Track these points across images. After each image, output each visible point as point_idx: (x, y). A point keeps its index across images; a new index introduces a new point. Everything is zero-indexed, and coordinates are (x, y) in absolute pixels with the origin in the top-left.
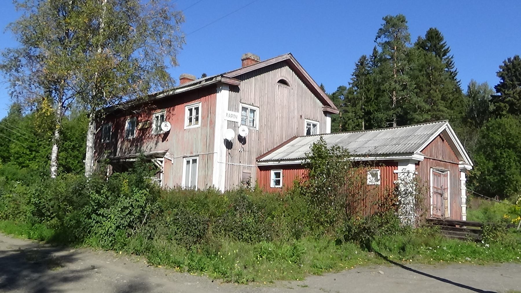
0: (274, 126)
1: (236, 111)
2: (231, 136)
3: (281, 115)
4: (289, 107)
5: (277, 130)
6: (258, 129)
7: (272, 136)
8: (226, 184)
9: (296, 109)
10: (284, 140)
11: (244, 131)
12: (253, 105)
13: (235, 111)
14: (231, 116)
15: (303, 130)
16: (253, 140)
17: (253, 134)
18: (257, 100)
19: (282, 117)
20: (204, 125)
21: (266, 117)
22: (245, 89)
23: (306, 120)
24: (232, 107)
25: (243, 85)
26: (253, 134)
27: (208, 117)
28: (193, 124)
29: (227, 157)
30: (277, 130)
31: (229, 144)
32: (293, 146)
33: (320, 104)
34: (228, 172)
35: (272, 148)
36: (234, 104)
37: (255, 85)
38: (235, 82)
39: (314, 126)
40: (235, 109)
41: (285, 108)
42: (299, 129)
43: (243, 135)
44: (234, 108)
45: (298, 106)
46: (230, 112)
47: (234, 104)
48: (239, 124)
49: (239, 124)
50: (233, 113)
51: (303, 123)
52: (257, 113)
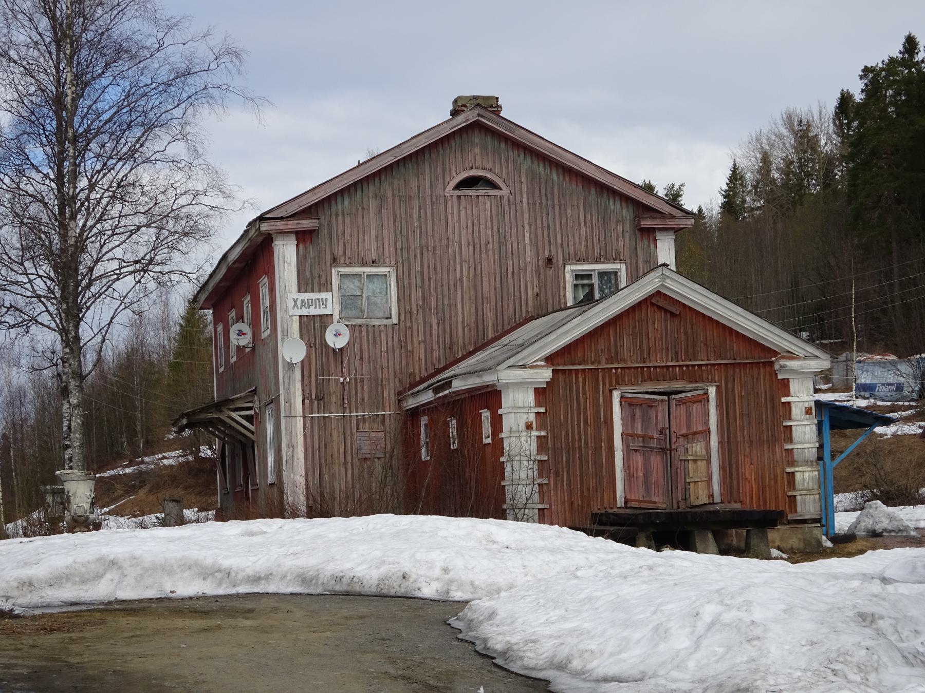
0: (452, 304)
3: (472, 271)
6: (395, 319)
7: (445, 331)
8: (310, 463)
9: (528, 248)
10: (491, 335)
11: (337, 334)
12: (374, 263)
13: (320, 291)
14: (303, 304)
16: (384, 348)
18: (389, 249)
19: (476, 278)
20: (271, 332)
21: (423, 287)
22: (348, 231)
23: (568, 268)
29: (307, 401)
30: (463, 312)
34: (313, 436)
35: (449, 360)
36: (316, 275)
37: (379, 214)
38: (305, 224)
40: (320, 284)
41: (487, 250)
42: (542, 295)
44: (316, 280)
45: (534, 236)
46: (306, 296)
47: (316, 275)
48: (336, 317)
49: (336, 317)
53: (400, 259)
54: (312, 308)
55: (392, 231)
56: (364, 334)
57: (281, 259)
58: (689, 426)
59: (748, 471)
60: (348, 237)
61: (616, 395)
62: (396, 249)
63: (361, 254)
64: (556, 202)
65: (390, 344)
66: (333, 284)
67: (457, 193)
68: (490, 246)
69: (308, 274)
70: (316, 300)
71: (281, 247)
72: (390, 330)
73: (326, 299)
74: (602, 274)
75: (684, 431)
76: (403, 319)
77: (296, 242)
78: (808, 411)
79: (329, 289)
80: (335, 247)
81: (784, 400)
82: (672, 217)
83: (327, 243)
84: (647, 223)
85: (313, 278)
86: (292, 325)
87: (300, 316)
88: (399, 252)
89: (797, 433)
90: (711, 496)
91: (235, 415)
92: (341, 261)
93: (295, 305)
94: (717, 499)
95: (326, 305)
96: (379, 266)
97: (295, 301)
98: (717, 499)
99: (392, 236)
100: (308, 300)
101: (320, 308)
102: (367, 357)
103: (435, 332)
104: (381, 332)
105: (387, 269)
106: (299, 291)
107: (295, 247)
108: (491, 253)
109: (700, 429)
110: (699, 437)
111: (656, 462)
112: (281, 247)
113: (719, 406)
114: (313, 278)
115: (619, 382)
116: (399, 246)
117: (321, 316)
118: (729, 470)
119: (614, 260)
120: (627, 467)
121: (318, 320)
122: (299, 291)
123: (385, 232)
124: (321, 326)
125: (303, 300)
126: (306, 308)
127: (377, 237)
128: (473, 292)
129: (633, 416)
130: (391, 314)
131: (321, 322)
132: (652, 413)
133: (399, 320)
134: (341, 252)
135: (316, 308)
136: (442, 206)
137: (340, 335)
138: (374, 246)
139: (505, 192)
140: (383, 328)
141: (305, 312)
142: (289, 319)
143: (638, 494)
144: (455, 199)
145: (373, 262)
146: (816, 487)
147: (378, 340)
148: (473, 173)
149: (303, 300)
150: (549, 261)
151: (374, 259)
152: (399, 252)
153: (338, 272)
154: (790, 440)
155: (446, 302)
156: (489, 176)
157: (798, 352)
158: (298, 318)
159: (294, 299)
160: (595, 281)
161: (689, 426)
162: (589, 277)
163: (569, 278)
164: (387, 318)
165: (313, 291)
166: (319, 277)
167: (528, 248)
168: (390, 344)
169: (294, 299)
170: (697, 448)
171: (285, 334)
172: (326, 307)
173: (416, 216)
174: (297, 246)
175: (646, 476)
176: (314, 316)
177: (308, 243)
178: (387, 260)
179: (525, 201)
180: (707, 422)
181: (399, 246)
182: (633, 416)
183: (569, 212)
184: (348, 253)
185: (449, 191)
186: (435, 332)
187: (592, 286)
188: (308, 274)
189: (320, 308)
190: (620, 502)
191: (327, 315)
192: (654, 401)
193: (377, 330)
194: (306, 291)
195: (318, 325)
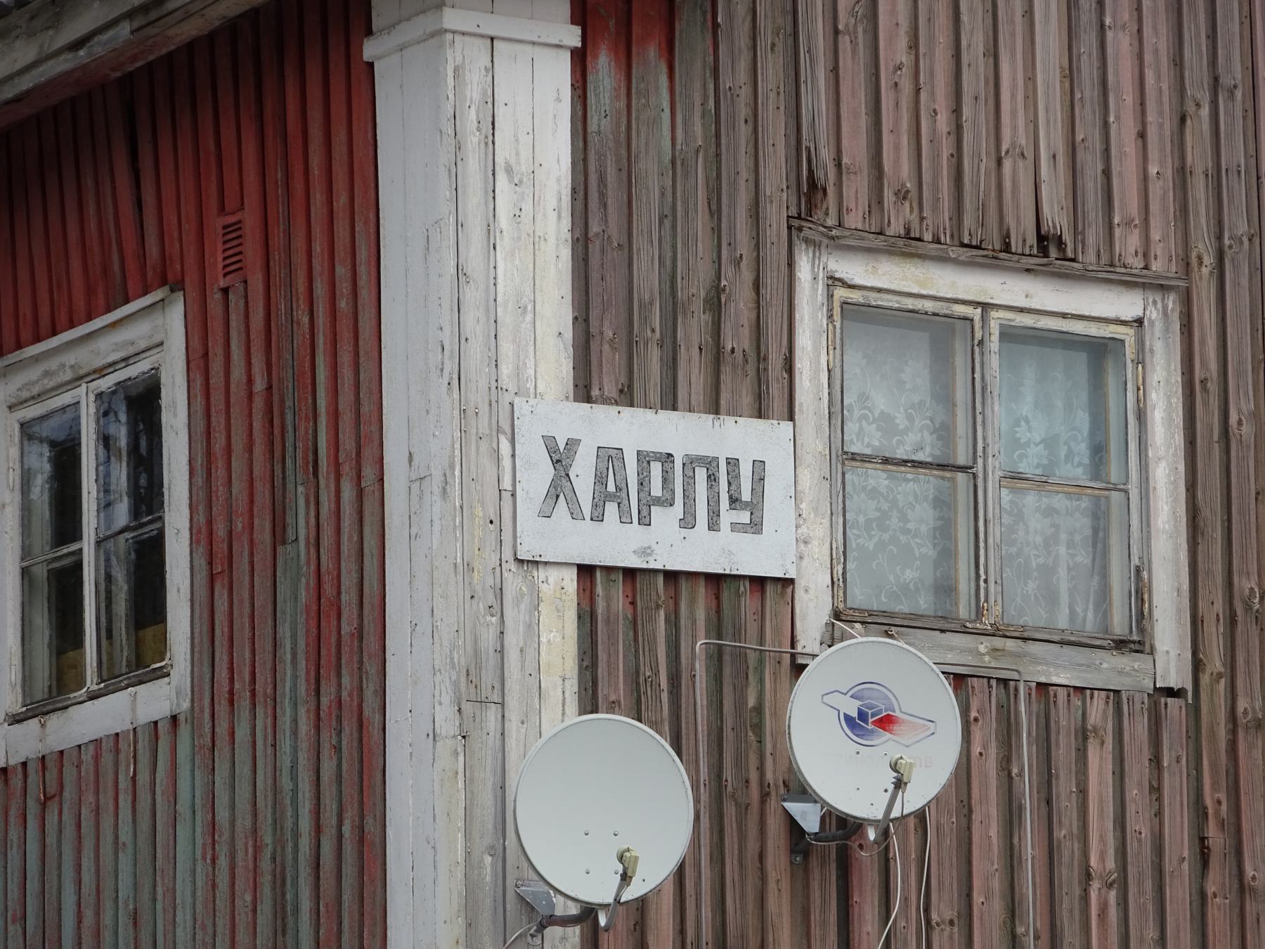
1: (736, 386)
13: (714, 408)
16: (1102, 858)
17: (1099, 761)
26: (1099, 761)
27: (279, 534)
28: (91, 682)
36: (695, 287)
40: (716, 356)
44: (694, 329)
47: (695, 287)
53: (1203, 247)
54: (666, 519)
55: (1158, 40)
57: (473, 141)
60: (895, 51)
62: (1182, 173)
63: (977, 168)
65: (1139, 824)
66: (803, 364)
70: (692, 462)
71: (477, 54)
72: (1137, 730)
73: (759, 466)
76: (1215, 662)
77: (573, 37)
79: (776, 392)
80: (816, 99)
83: (772, 70)
85: (674, 311)
86: (533, 628)
87: (586, 572)
88: (1199, 191)
93: (560, 488)
95: (755, 507)
96: (1085, 278)
97: (561, 457)
99: (1159, 82)
100: (644, 459)
101: (713, 526)
102: (997, 908)
104: (1083, 734)
105: (1127, 305)
106: (584, 392)
107: (559, 72)
112: (472, 55)
114: (674, 311)
116: (1198, 158)
117: (715, 580)
121: (697, 608)
122: (584, 392)
123: (1121, 44)
124: (716, 657)
125: (610, 458)
126: (625, 518)
127: (1071, 75)
130: (1142, 615)
131: (717, 627)
133: (1197, 666)
134: (856, 149)
135: (688, 522)
137: (886, 722)
138: (1052, 138)
140: (1097, 711)
142: (514, 581)
145: (1043, 240)
147: (1065, 786)
149: (610, 458)
151: (1056, 217)
152: (1199, 191)
153: (834, 281)
158: (570, 579)
159: (550, 444)
164: (1121, 645)
165: (670, 402)
166: (716, 302)
168: (1139, 824)
169: (550, 444)
172: (755, 526)
174: (580, 59)
176: (672, 577)
177: (650, 55)
178: (1128, 244)
181: (1198, 158)
184: (898, 164)
188: (648, 277)
189: (713, 526)
191: (759, 583)
193: (1064, 719)
194: (627, 396)
195: (698, 645)
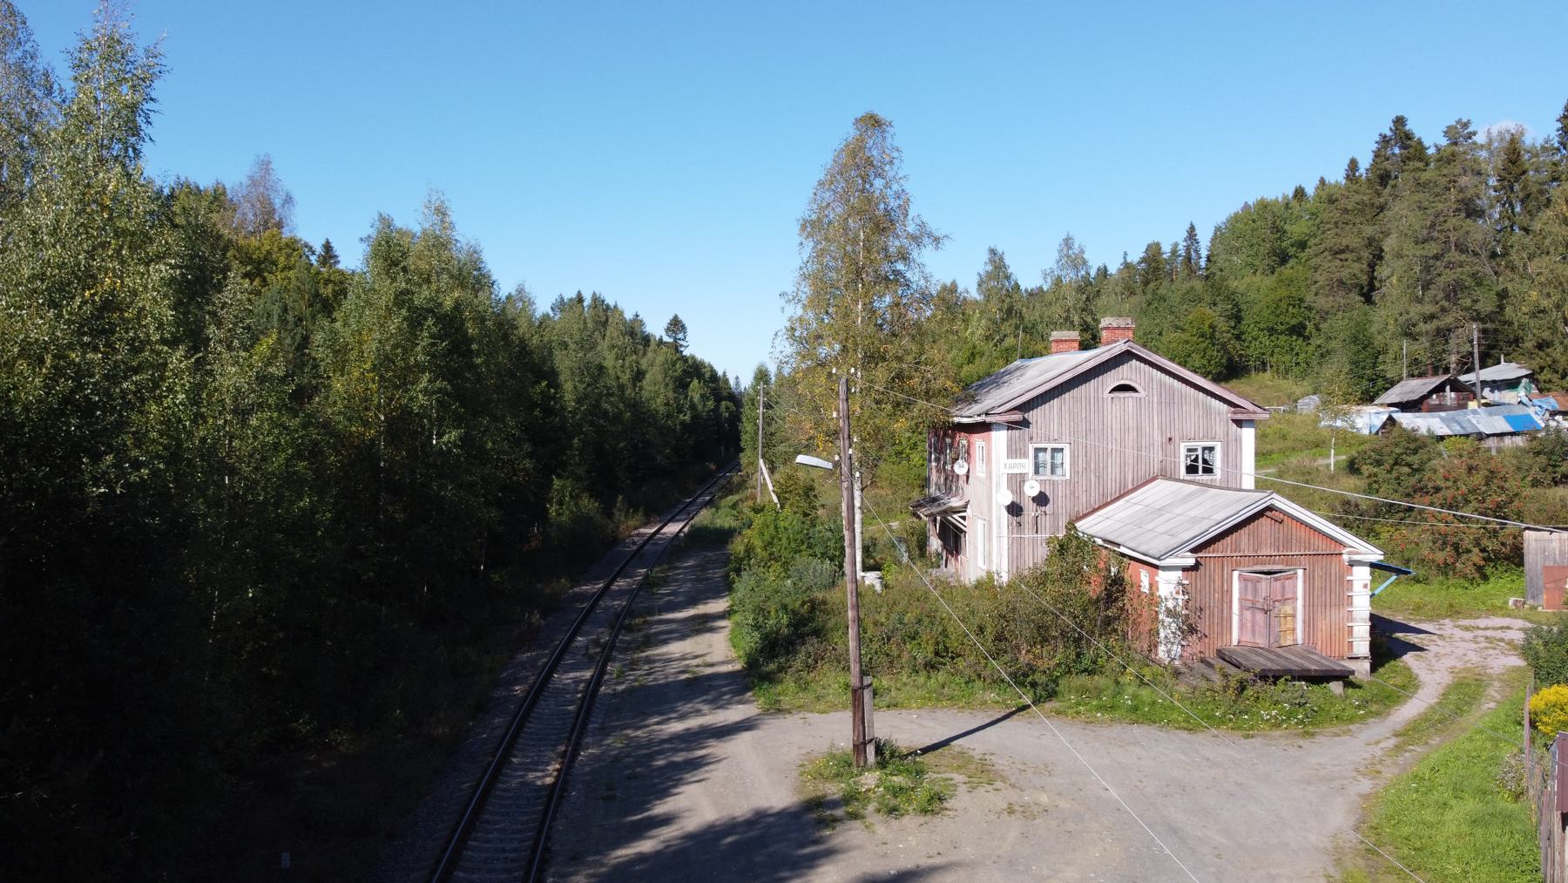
2: (1008, 498)
4: (1139, 429)
5: (1113, 471)
6: (1068, 477)
10: (1130, 487)
15: (1176, 464)
18: (1066, 431)
23: (1182, 445)
24: (1014, 451)
25: (1032, 416)
30: (1113, 471)
31: (1015, 510)
32: (1128, 501)
33: (1225, 407)
38: (1017, 417)
39: (1211, 449)
43: (1035, 493)
50: (1018, 461)
51: (1176, 453)
52: (1067, 452)
56: (1047, 486)
58: (1283, 595)
59: (1322, 624)
61: (1236, 574)
64: (1176, 401)
67: (1112, 395)
68: (1131, 430)
69: (1014, 447)
74: (1204, 449)
75: (1279, 598)
78: (1365, 586)
81: (1349, 578)
82: (1255, 413)
84: (1239, 417)
89: (1355, 600)
90: (1295, 640)
91: (955, 516)
92: (1034, 440)
94: (1300, 642)
98: (1300, 642)
103: (1093, 485)
108: (1131, 435)
109: (1290, 596)
110: (1290, 601)
111: (1260, 617)
113: (1305, 582)
115: (1238, 564)
118: (1310, 624)
119: (1213, 439)
120: (1241, 620)
128: (1118, 461)
129: (1246, 589)
132: (1259, 585)
136: (1101, 404)
139: (1142, 394)
141: (1011, 471)
143: (1248, 638)
144: (1110, 399)
146: (1368, 635)
148: (1122, 382)
150: (1170, 439)
154: (1351, 604)
155: (1101, 465)
156: (1133, 384)
157: (1362, 549)
160: (1200, 452)
161: (1283, 595)
162: (1196, 450)
163: (1183, 452)
167: (1156, 431)
170: (1288, 609)
171: (998, 484)
173: (1084, 410)
175: (1253, 626)
179: (1155, 400)
180: (1295, 593)
182: (1246, 589)
183: (1184, 408)
185: (1106, 394)
186: (1093, 485)
187: (1197, 456)
190: (1235, 642)
192: (1261, 578)
